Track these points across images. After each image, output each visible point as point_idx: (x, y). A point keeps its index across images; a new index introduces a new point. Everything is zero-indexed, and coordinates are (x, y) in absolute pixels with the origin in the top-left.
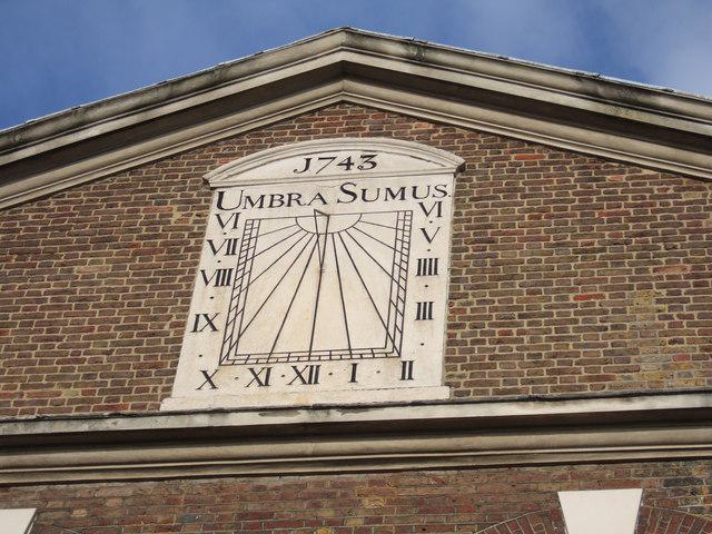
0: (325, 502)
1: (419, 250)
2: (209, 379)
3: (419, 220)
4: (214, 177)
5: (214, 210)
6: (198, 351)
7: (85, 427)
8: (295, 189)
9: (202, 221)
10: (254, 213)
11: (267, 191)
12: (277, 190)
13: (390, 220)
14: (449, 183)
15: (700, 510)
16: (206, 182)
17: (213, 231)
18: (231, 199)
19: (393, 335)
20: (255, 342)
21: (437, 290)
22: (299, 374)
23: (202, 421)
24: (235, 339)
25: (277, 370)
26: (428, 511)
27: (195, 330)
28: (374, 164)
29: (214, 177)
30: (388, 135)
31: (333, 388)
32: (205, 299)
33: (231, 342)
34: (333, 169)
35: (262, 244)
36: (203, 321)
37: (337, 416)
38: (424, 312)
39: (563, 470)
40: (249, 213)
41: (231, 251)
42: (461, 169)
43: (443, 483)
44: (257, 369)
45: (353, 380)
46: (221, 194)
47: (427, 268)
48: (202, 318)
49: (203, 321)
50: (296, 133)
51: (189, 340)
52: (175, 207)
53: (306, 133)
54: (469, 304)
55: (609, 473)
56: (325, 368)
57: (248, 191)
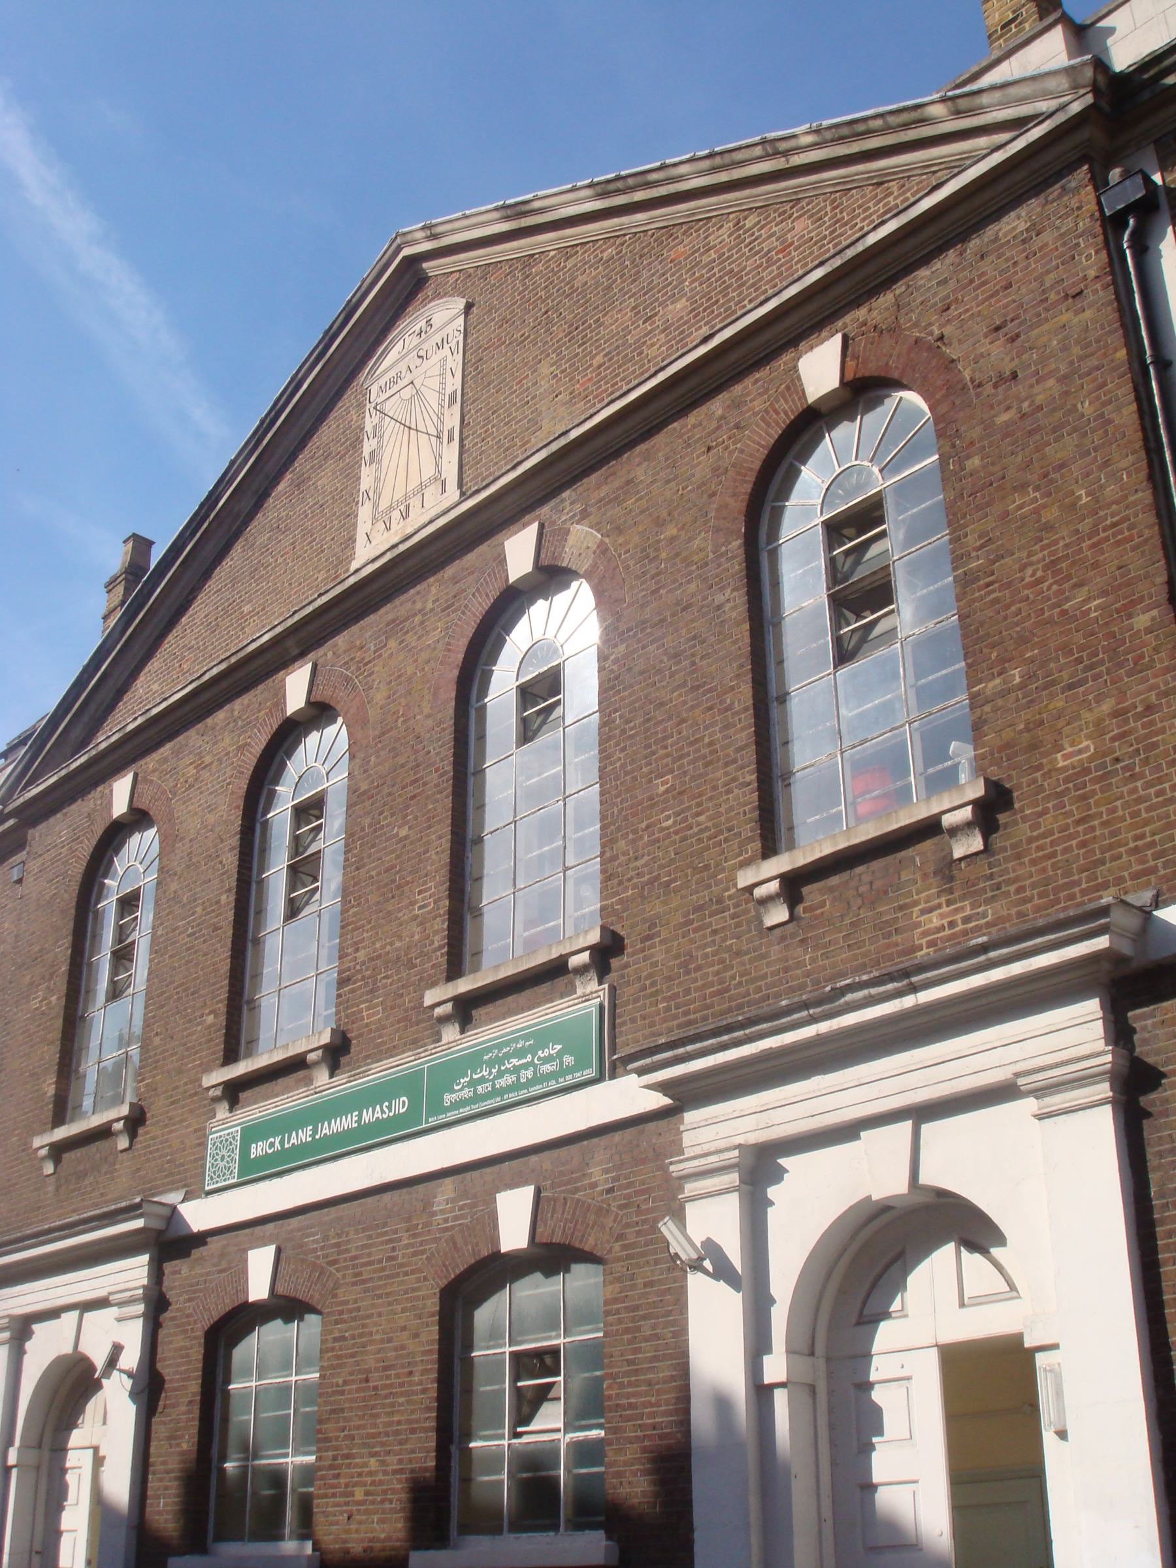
42: (469, 307)
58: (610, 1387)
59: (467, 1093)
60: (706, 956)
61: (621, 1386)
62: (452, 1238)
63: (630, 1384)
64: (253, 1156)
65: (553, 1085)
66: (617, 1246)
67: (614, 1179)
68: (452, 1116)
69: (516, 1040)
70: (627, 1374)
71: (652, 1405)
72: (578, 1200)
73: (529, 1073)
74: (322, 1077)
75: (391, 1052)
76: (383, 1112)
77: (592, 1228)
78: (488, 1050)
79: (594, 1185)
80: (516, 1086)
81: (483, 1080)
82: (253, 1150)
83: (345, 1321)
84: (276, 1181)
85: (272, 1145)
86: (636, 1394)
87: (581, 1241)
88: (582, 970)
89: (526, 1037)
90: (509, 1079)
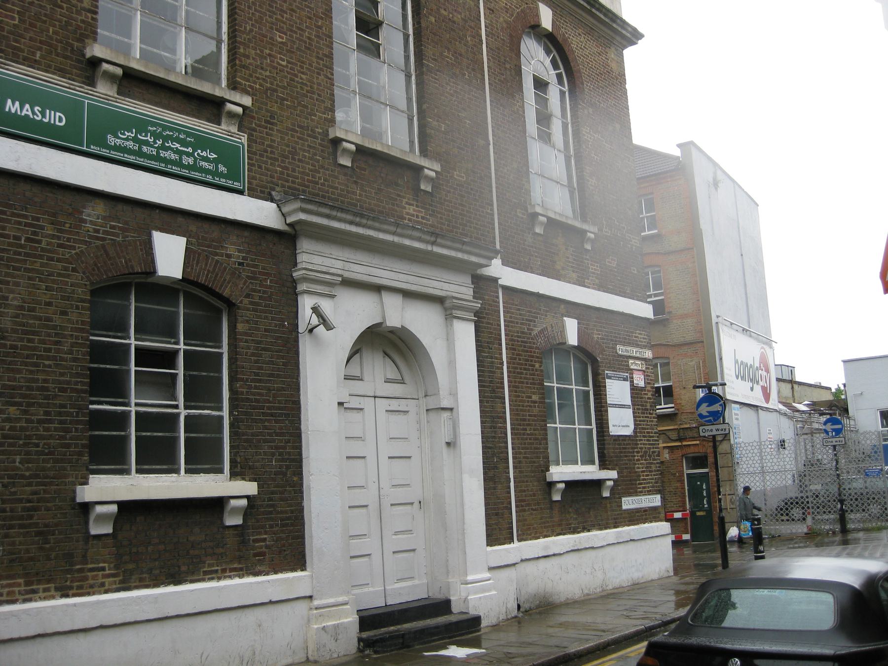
58: (241, 387)
59: (130, 144)
60: (305, 157)
61: (250, 387)
62: (103, 246)
63: (256, 387)
65: (185, 172)
66: (246, 301)
67: (244, 258)
68: (104, 152)
69: (179, 131)
70: (253, 381)
71: (270, 402)
72: (217, 261)
73: (191, 161)
75: (33, 63)
76: (34, 113)
77: (229, 283)
79: (229, 256)
80: (179, 164)
81: (147, 143)
86: (259, 394)
87: (220, 289)
88: (232, 115)
89: (188, 134)
90: (173, 157)
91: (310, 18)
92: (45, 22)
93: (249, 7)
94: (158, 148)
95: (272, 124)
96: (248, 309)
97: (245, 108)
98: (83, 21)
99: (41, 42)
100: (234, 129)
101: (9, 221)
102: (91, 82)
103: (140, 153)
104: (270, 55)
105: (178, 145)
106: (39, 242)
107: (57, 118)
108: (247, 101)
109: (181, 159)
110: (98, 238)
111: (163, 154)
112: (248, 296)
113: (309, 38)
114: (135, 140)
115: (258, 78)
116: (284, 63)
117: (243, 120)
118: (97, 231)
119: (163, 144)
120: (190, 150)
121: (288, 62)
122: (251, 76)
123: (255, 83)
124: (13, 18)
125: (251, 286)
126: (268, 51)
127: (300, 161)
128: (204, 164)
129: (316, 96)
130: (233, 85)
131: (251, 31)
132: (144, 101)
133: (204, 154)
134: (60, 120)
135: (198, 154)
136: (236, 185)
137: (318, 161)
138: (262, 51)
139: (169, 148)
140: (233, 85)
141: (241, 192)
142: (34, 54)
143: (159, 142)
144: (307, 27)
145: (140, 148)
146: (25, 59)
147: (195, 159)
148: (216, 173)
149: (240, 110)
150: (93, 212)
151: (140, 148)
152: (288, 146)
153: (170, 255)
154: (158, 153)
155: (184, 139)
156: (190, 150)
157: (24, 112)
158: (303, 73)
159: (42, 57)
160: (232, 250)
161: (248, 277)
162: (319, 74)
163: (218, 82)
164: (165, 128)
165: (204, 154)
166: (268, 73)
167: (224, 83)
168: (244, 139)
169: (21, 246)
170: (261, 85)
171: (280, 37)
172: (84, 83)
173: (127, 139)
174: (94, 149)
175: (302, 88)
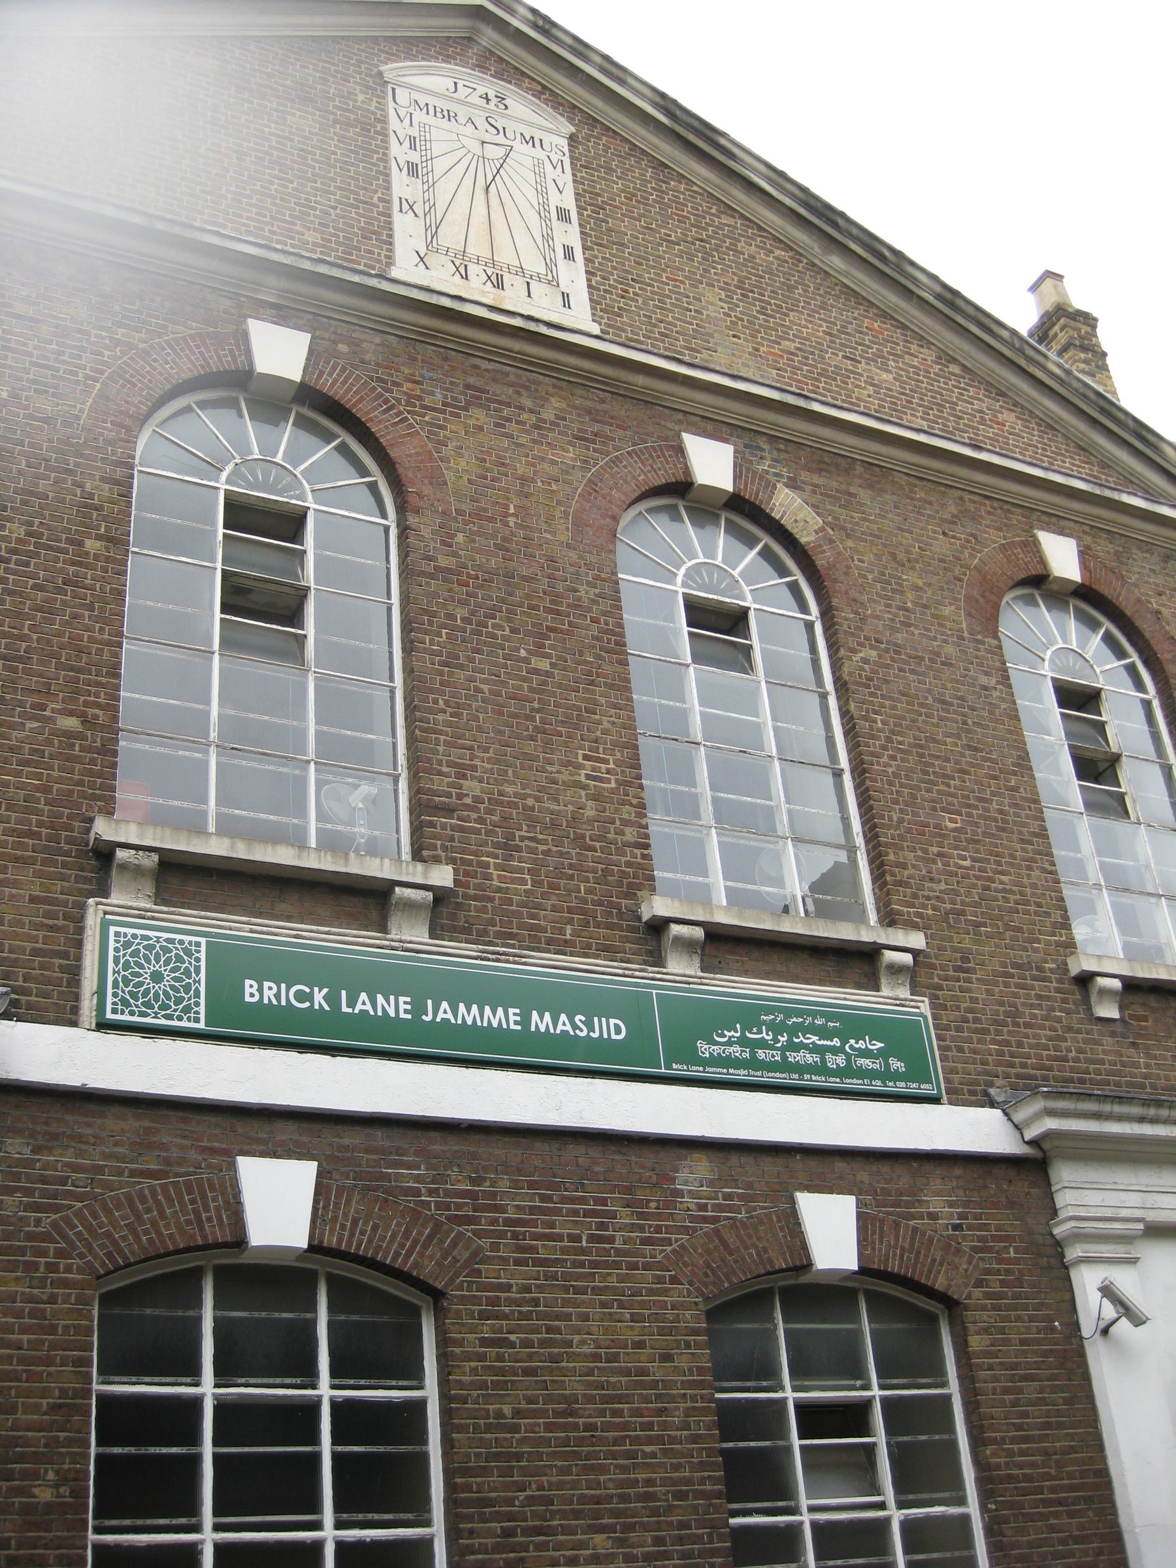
0: (524, 393)
1: (555, 200)
2: (422, 259)
3: (550, 172)
4: (390, 70)
5: (391, 104)
6: (407, 234)
7: (356, 279)
8: (454, 107)
9: (382, 108)
10: (430, 119)
11: (433, 102)
12: (440, 104)
13: (529, 162)
14: (564, 143)
15: (767, 472)
16: (380, 74)
17: (393, 123)
18: (402, 95)
19: (551, 265)
20: (450, 237)
21: (571, 235)
22: (489, 278)
23: (446, 302)
24: (434, 230)
25: (473, 269)
26: (598, 422)
27: (401, 211)
28: (506, 107)
29: (390, 70)
30: (510, 82)
31: (513, 298)
32: (401, 186)
33: (433, 232)
34: (475, 99)
35: (437, 149)
36: (405, 207)
37: (544, 330)
38: (569, 254)
39: (680, 416)
40: (419, 116)
41: (413, 146)
43: (603, 401)
44: (457, 263)
45: (529, 296)
46: (394, 89)
47: (563, 215)
48: (404, 201)
49: (405, 207)
50: (440, 54)
51: (397, 218)
52: (358, 88)
53: (448, 56)
54: (597, 257)
55: (709, 427)
56: (506, 277)
57: (415, 95)
58: (994, 1454)
60: (1034, 1016)
61: (1011, 1453)
62: (717, 1232)
63: (1022, 1453)
64: (248, 999)
65: (834, 1082)
66: (977, 1292)
67: (961, 1216)
68: (696, 1071)
69: (814, 1014)
70: (1013, 1440)
71: (1052, 1478)
72: (915, 1229)
73: (841, 1060)
74: (411, 933)
75: (562, 947)
76: (575, 1027)
77: (941, 1264)
78: (769, 1010)
79: (933, 1216)
80: (821, 1069)
81: (762, 1044)
82: (248, 991)
83: (506, 1317)
84: (292, 1056)
85: (310, 997)
87: (928, 1277)
88: (896, 970)
89: (830, 1017)
90: (811, 1058)
91: (995, 778)
92: (571, 877)
93: (891, 784)
94: (783, 1049)
95: (967, 971)
96: (984, 1308)
97: (915, 953)
98: (629, 864)
99: (570, 910)
100: (904, 993)
101: (558, 1212)
102: (657, 959)
103: (753, 1064)
104: (939, 855)
105: (815, 1038)
106: (611, 1240)
107: (612, 1028)
108: (917, 940)
109: (823, 1060)
110: (705, 1219)
111: (792, 1057)
112: (979, 1283)
113: (1001, 812)
114: (743, 1042)
115: (928, 898)
116: (967, 863)
117: (918, 973)
118: (703, 1207)
119: (790, 1040)
120: (836, 1042)
121: (974, 860)
122: (915, 896)
123: (924, 907)
124: (523, 882)
125: (981, 1265)
126: (935, 849)
127: (1027, 1025)
128: (862, 1062)
129: (1033, 908)
130: (889, 919)
131: (901, 821)
132: (746, 973)
133: (861, 1045)
134: (618, 1032)
135: (851, 1047)
136: (926, 1089)
137: (1059, 1020)
138: (925, 851)
139: (802, 1046)
140: (889, 919)
141: (935, 1100)
142: (562, 931)
143: (783, 1039)
144: (993, 794)
145: (753, 1054)
146: (549, 942)
147: (848, 1056)
148: (887, 1075)
149: (907, 958)
150: (693, 1176)
151: (753, 1054)
152: (1002, 1004)
153: (831, 1231)
154: (784, 1057)
155: (824, 1026)
156: (836, 1042)
157: (560, 1027)
158: (1002, 873)
159: (575, 933)
160: (936, 1204)
161: (973, 1248)
162: (1029, 868)
163: (862, 918)
164: (789, 1013)
165: (861, 1045)
166: (943, 886)
167: (873, 917)
168: (925, 1007)
169: (583, 1251)
170: (935, 908)
171: (951, 820)
172: (645, 963)
173: (729, 1043)
174: (678, 1069)
175: (1006, 900)
